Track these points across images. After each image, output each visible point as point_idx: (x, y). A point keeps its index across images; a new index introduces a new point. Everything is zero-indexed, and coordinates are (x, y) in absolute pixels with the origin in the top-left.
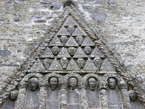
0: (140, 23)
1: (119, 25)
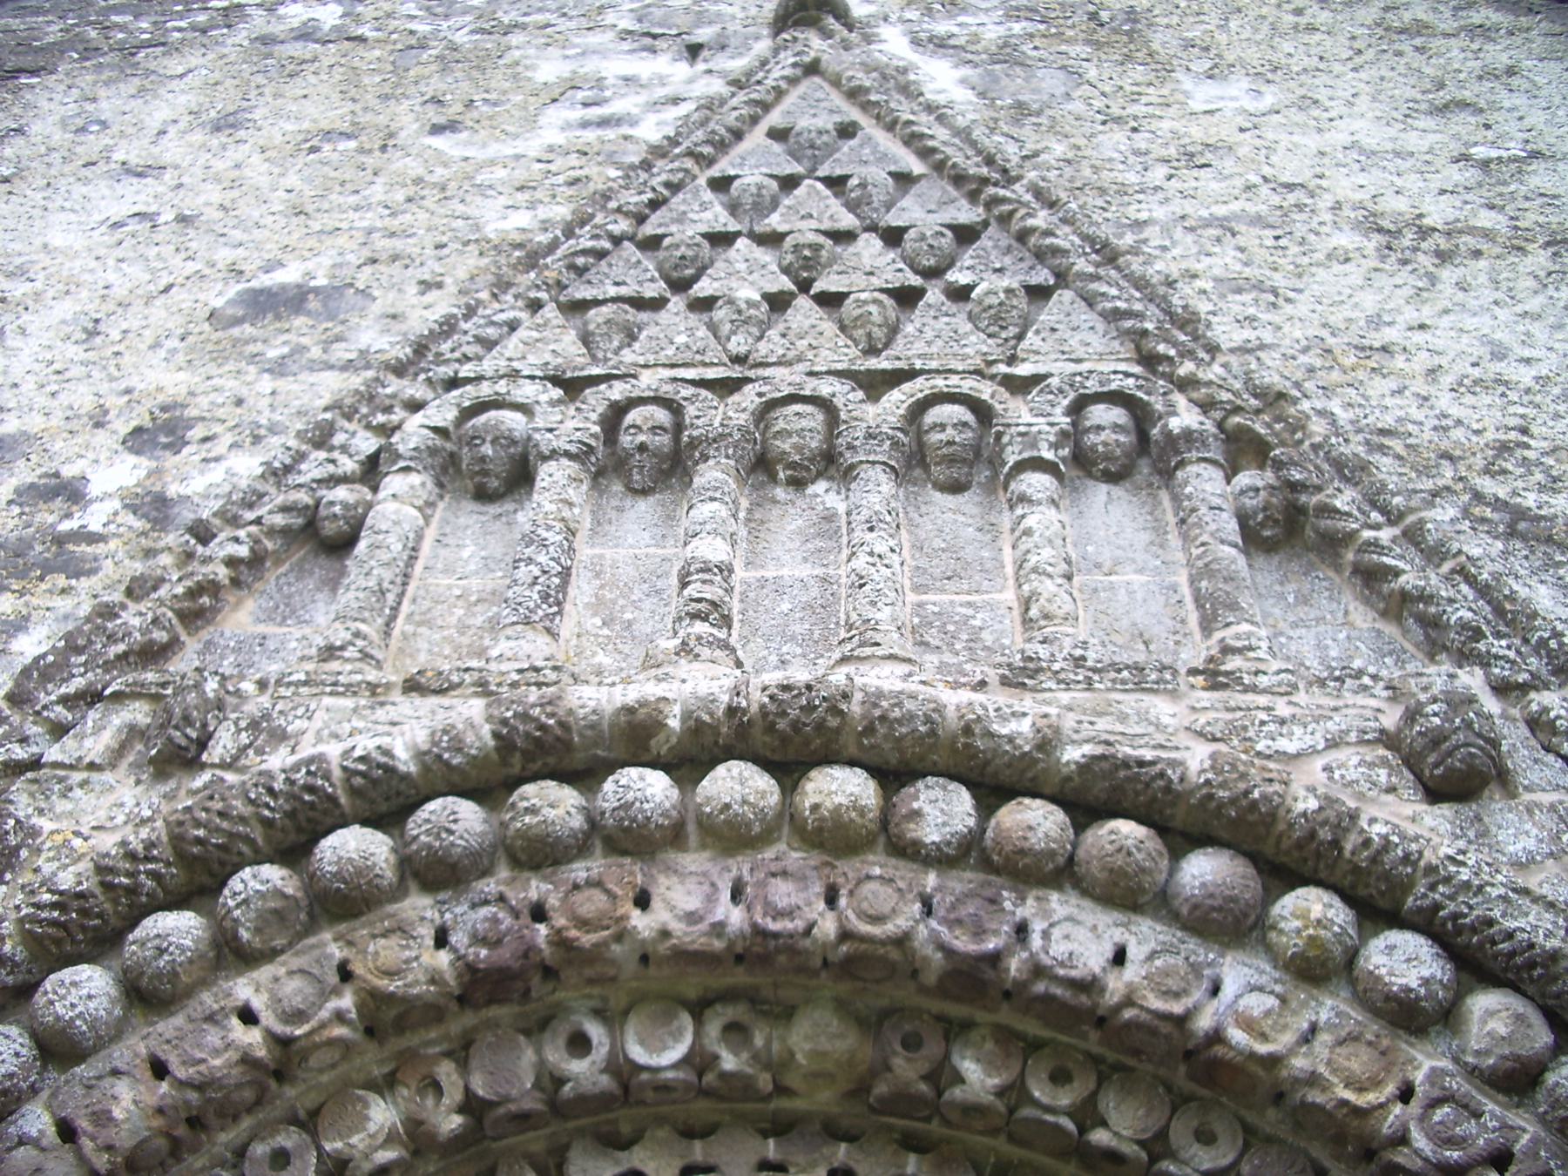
0: (1316, 113)
1: (1166, 125)
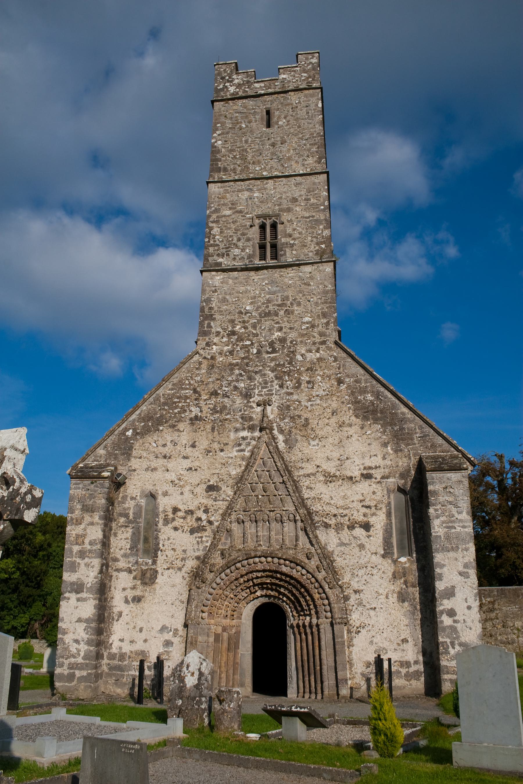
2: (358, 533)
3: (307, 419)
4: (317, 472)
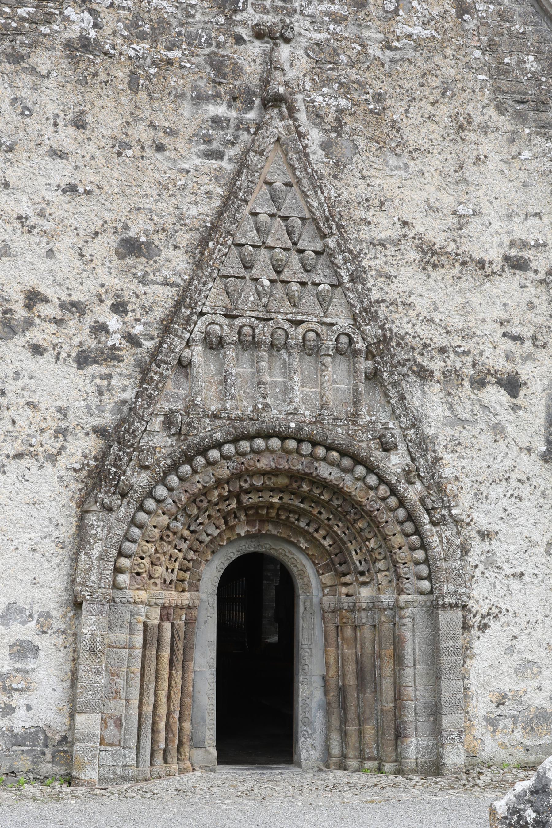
0: (422, 180)
1: (378, 181)
2: (493, 399)
3: (380, 94)
4: (405, 236)
